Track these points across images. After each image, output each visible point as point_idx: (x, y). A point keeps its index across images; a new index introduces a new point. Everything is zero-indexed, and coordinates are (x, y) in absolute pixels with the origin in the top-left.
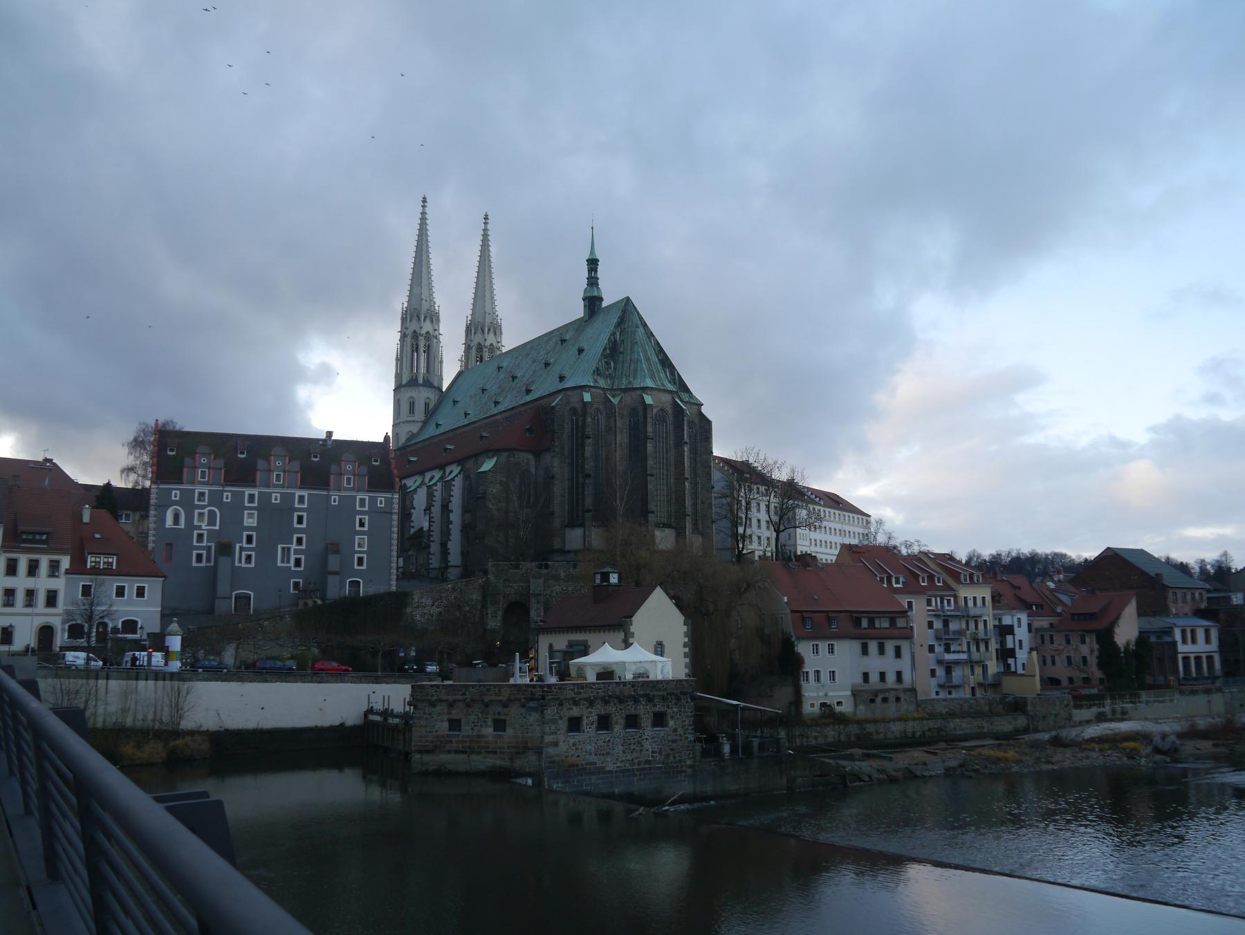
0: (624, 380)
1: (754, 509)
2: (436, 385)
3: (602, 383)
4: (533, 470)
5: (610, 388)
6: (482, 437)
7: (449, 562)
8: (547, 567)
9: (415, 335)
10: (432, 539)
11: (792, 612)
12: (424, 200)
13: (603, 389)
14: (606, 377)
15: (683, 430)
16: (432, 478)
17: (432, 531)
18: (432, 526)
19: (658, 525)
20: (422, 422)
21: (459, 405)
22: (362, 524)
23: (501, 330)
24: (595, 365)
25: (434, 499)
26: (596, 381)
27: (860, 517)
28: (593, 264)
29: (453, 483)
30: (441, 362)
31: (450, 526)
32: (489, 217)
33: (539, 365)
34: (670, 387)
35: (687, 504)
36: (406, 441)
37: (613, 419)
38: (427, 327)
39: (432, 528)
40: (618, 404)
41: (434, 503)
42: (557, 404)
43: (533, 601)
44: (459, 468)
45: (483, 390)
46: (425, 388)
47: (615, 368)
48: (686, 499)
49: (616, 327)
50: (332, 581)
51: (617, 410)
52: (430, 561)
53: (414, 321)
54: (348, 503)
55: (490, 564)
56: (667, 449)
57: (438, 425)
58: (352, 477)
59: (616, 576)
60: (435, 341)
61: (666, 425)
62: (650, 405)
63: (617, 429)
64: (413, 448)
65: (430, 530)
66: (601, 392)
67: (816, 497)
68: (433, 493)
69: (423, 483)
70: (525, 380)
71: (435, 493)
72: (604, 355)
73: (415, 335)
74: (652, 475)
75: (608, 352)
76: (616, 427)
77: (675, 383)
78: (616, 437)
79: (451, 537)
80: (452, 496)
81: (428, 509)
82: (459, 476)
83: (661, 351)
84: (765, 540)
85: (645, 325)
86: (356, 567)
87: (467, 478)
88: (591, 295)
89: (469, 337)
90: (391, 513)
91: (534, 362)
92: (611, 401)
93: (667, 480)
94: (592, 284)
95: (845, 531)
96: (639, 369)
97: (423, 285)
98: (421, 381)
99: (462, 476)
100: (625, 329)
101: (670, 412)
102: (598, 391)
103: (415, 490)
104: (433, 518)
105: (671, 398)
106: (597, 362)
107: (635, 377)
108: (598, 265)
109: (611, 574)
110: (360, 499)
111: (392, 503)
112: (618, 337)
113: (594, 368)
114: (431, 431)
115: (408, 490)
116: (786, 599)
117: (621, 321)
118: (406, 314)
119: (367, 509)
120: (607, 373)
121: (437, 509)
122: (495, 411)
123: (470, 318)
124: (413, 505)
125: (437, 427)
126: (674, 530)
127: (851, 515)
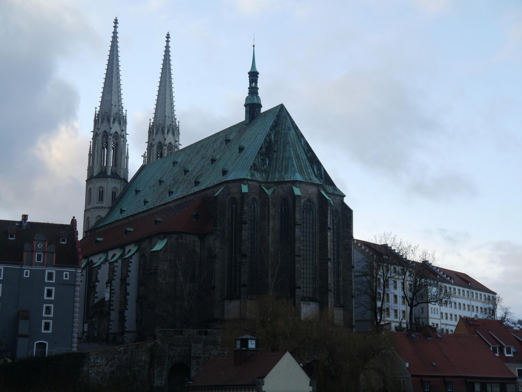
0: (277, 174)
1: (391, 287)
2: (122, 177)
3: (258, 176)
4: (198, 250)
5: (265, 181)
6: (156, 222)
7: (126, 327)
8: (206, 333)
9: (106, 135)
10: (112, 308)
11: (413, 376)
12: (116, 22)
13: (258, 182)
14: (261, 172)
15: (327, 217)
16: (114, 255)
17: (113, 301)
18: (112, 297)
19: (304, 299)
20: (109, 208)
21: (141, 194)
22: (49, 293)
23: (178, 131)
24: (252, 162)
25: (115, 274)
26: (252, 175)
27: (487, 294)
28: (253, 76)
29: (131, 260)
30: (127, 157)
31: (128, 297)
32: (170, 36)
33: (207, 161)
34: (316, 181)
35: (329, 281)
36: (95, 224)
37: (267, 207)
38: (115, 128)
39: (112, 299)
40: (272, 195)
41: (114, 277)
42: (219, 194)
43: (194, 362)
44: (136, 248)
45: (161, 182)
46: (113, 180)
47: (269, 165)
48: (329, 276)
49: (271, 130)
50: (22, 342)
51: (270, 199)
52: (110, 327)
53: (105, 123)
54: (37, 276)
55: (158, 330)
56: (313, 233)
57: (122, 211)
58: (42, 254)
59: (254, 342)
60: (122, 139)
61: (313, 214)
62: (298, 196)
63: (270, 216)
64: (101, 230)
65: (110, 300)
66: (257, 184)
67: (447, 276)
68: (114, 269)
69: (106, 260)
70: (194, 173)
71: (116, 269)
72: (260, 153)
73: (106, 135)
74: (299, 256)
75: (264, 150)
76: (269, 214)
77: (321, 178)
78: (269, 223)
79: (128, 307)
80: (130, 271)
81: (109, 282)
82: (136, 254)
83: (310, 150)
84: (401, 313)
85: (296, 128)
86: (43, 331)
87: (142, 256)
88: (252, 102)
89: (151, 136)
90: (75, 285)
91: (203, 158)
92: (265, 192)
93: (313, 260)
94: (253, 93)
95: (473, 307)
96: (290, 165)
97: (113, 93)
98: (109, 173)
99: (138, 254)
100: (279, 131)
101: (316, 202)
102: (255, 183)
103: (99, 266)
104: (113, 290)
105: (317, 190)
106: (254, 159)
107: (286, 172)
108: (258, 77)
109: (249, 341)
110: (49, 273)
111: (76, 277)
112: (273, 138)
113: (251, 164)
114: (117, 216)
115: (94, 266)
116: (407, 365)
117: (276, 125)
118: (98, 117)
119: (54, 281)
120: (262, 168)
121: (116, 283)
122: (169, 199)
123: (152, 121)
124: (97, 278)
125: (121, 213)
126: (318, 303)
127: (479, 292)
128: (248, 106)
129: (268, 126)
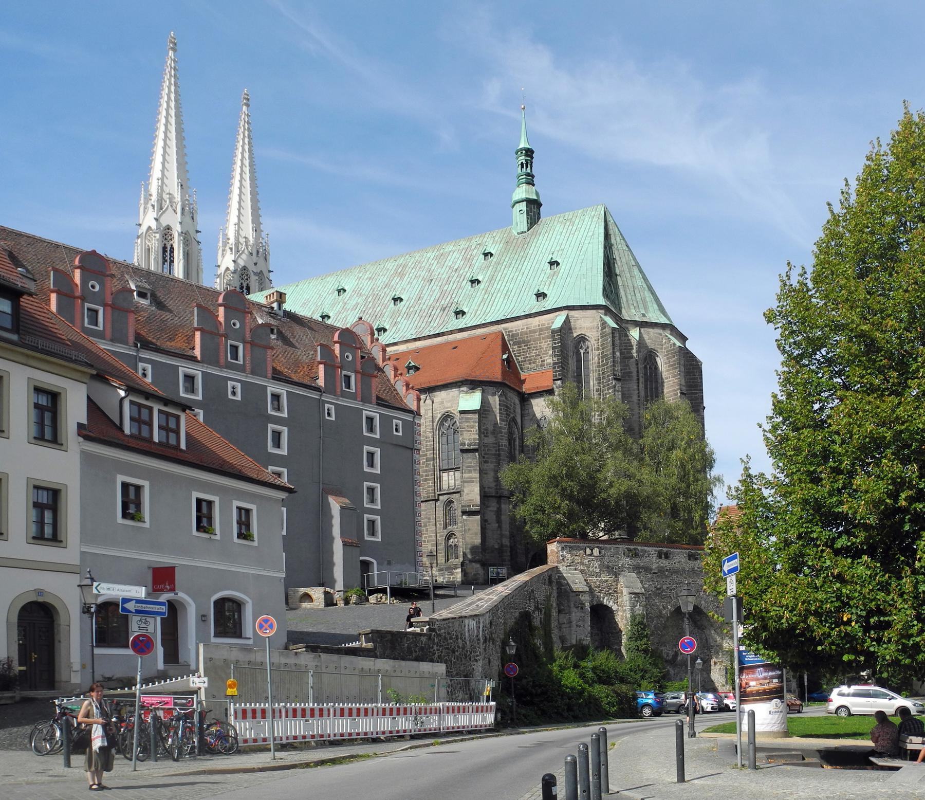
0: (633, 311)
78: (638, 386)
128: (525, 203)
129: (596, 232)
